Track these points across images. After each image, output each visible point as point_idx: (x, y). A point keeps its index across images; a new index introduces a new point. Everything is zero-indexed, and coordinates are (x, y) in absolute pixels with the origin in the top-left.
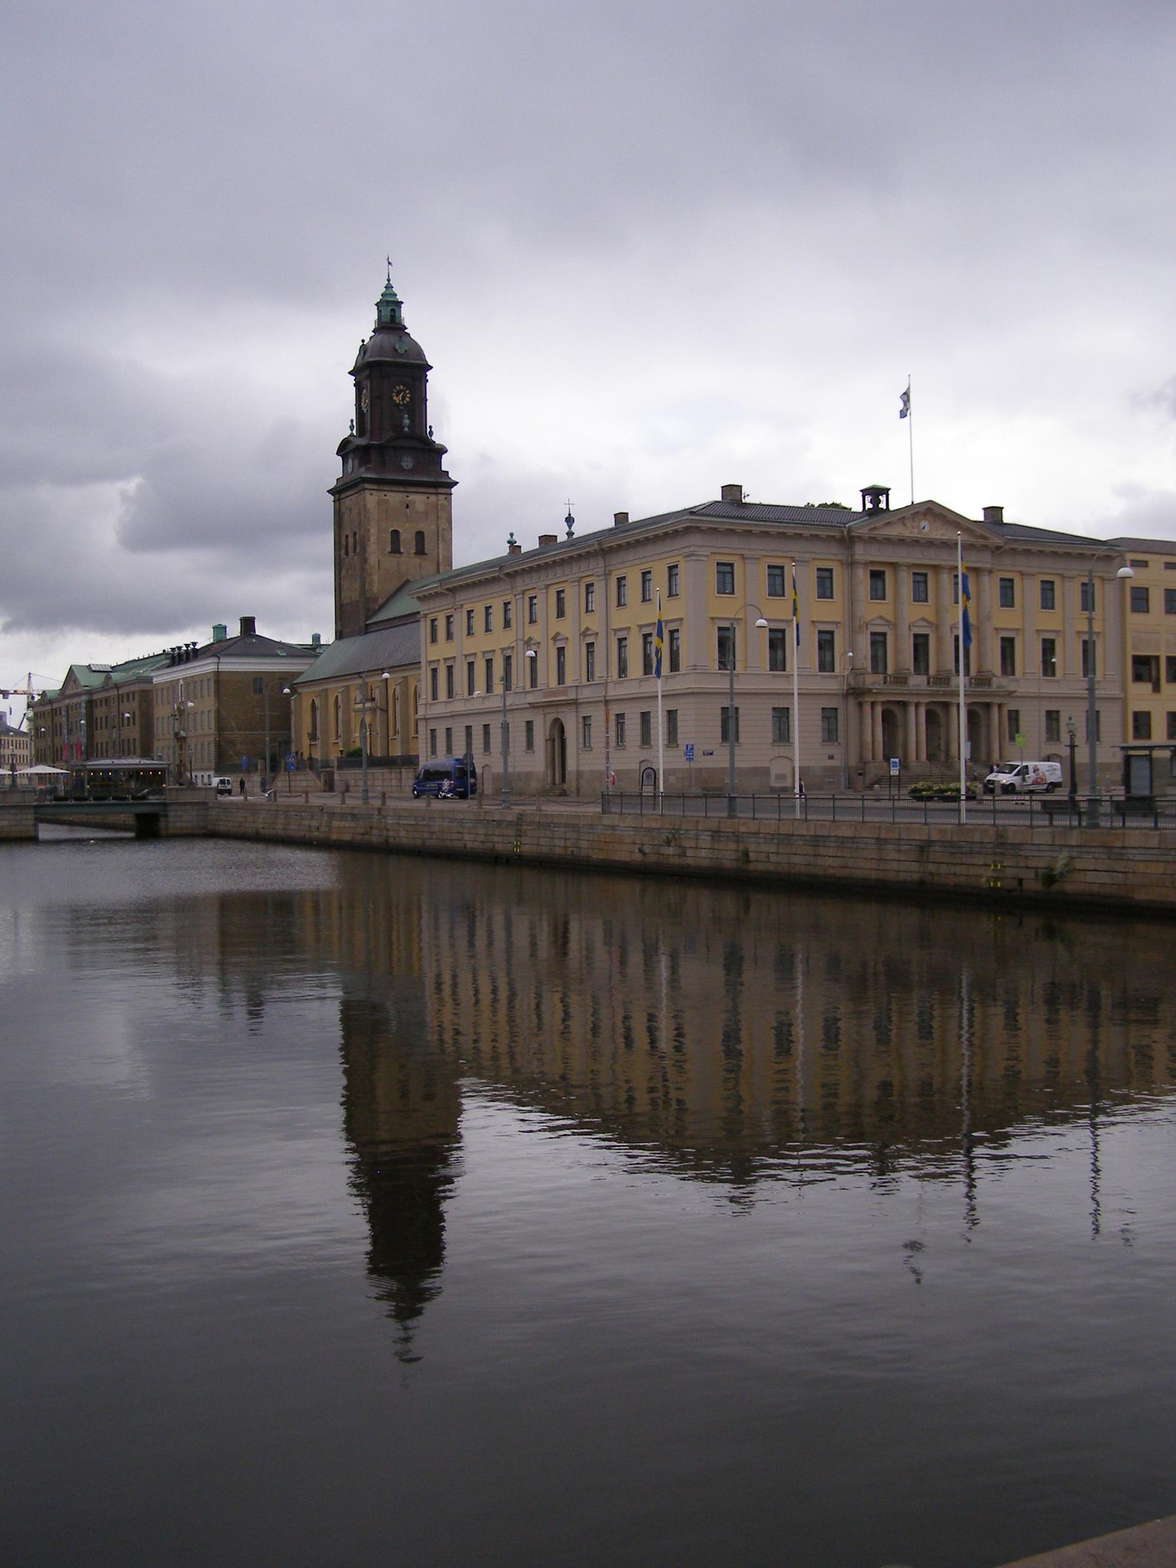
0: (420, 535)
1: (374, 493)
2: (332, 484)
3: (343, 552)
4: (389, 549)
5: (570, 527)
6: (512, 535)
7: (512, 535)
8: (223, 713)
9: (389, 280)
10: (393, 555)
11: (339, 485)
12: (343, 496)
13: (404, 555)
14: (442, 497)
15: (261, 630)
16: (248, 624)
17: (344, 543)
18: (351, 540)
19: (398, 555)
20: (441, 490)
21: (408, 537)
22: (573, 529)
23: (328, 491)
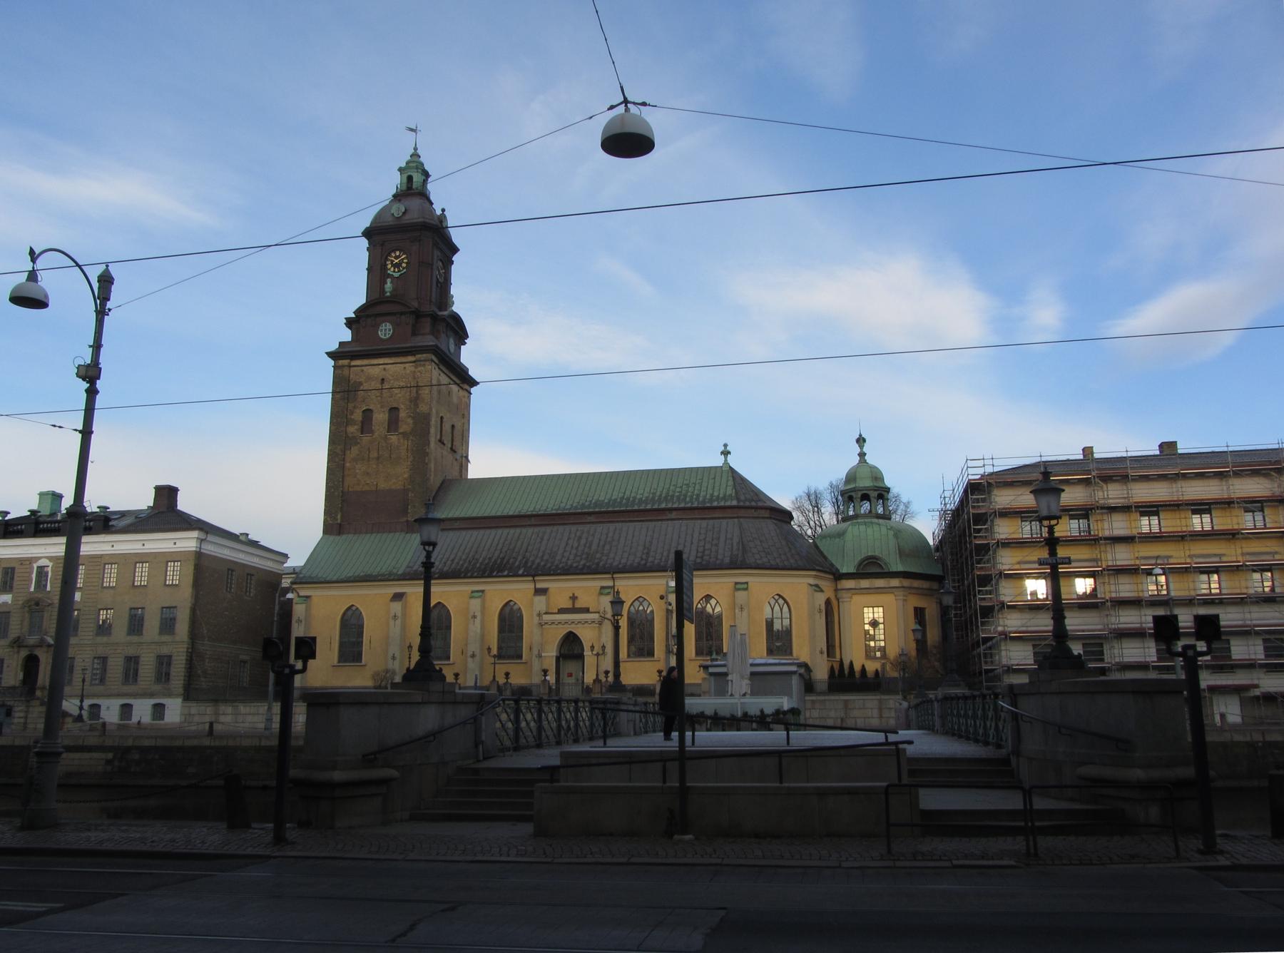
0: (453, 426)
1: (436, 367)
2: (334, 347)
3: (353, 429)
4: (438, 437)
5: (861, 447)
6: (725, 446)
7: (725, 446)
8: (198, 612)
9: (416, 149)
10: (440, 443)
11: (341, 350)
12: (354, 363)
13: (445, 448)
14: (466, 394)
15: (183, 504)
16: (167, 495)
17: (358, 416)
18: (380, 417)
19: (442, 446)
20: (466, 386)
21: (447, 427)
22: (865, 450)
23: (327, 353)
